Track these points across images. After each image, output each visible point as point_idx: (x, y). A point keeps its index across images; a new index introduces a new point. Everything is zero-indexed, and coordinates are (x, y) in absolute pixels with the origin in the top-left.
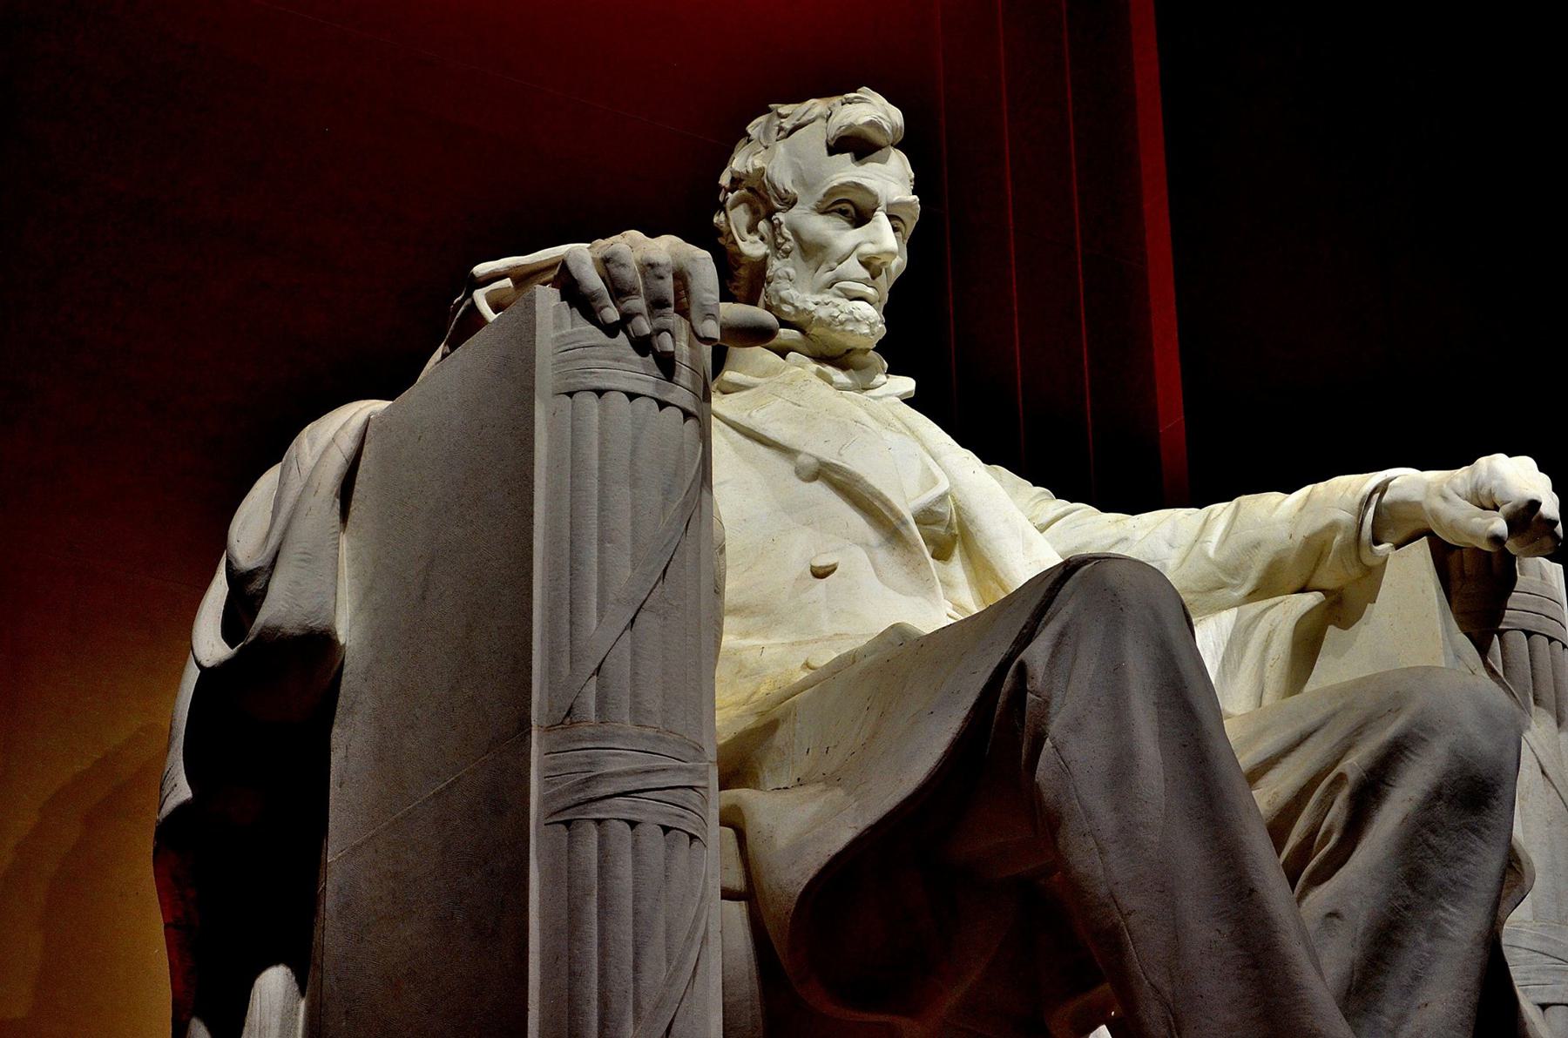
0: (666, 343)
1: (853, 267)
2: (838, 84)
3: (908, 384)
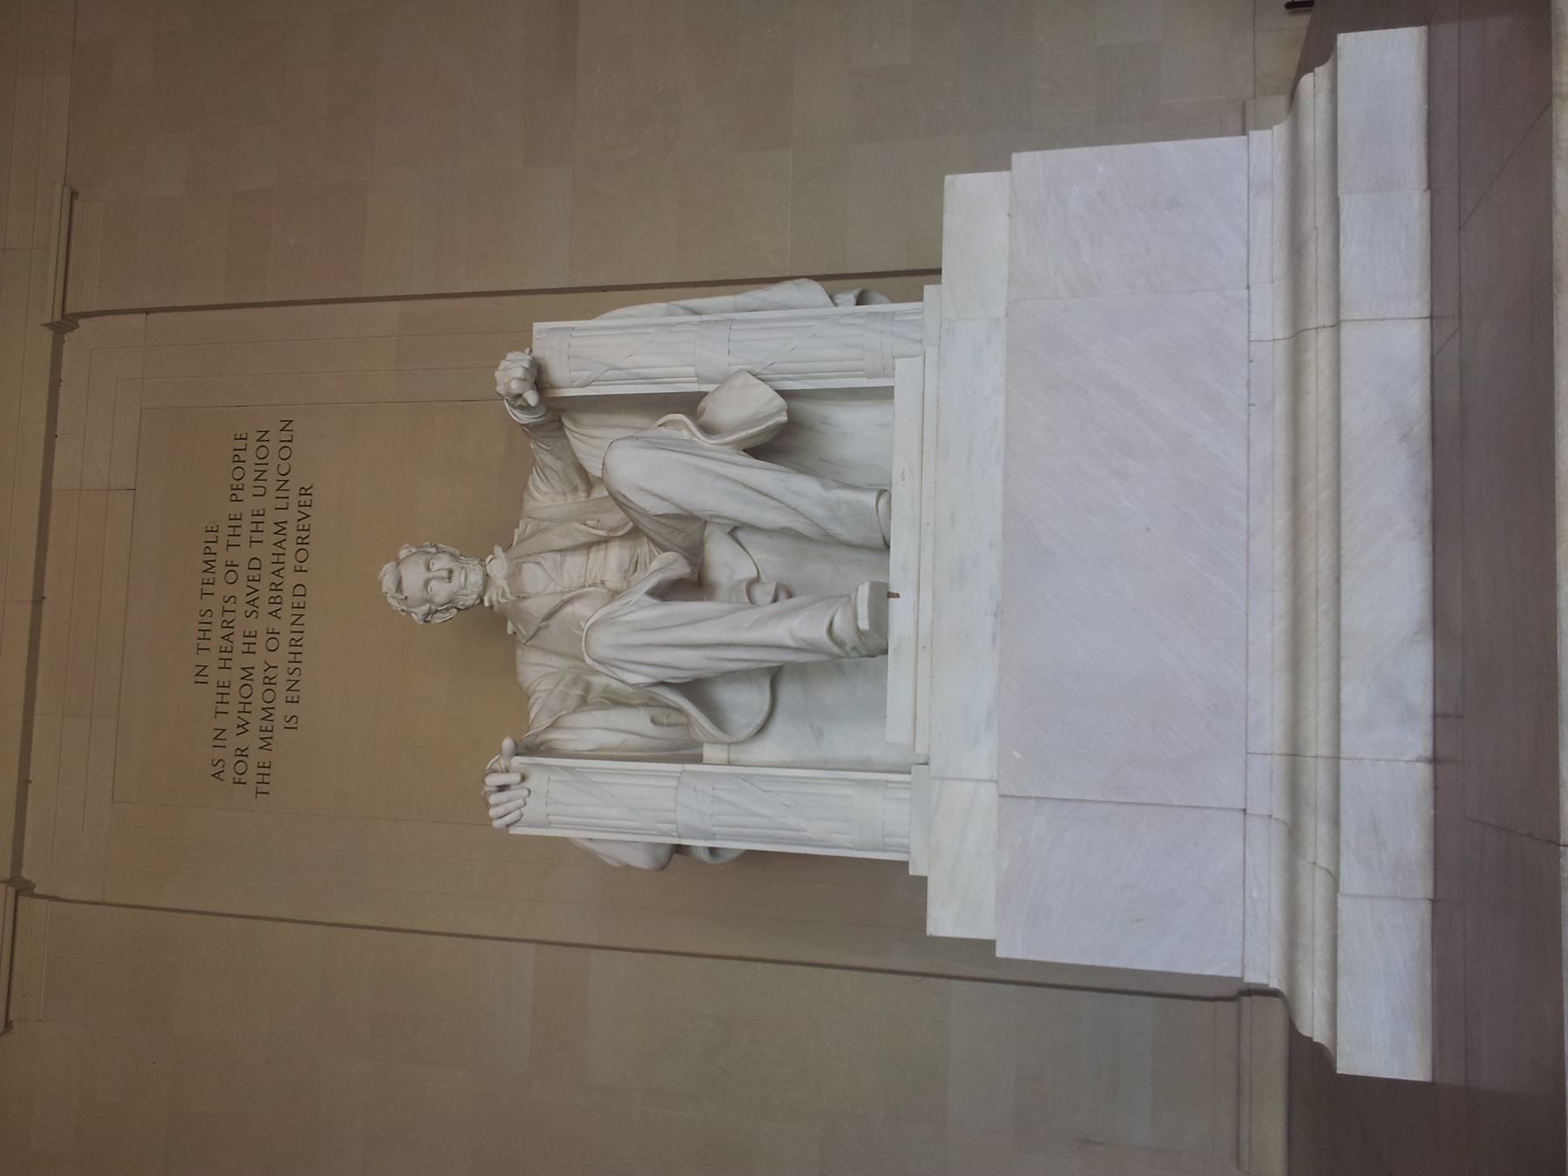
3: (498, 550)
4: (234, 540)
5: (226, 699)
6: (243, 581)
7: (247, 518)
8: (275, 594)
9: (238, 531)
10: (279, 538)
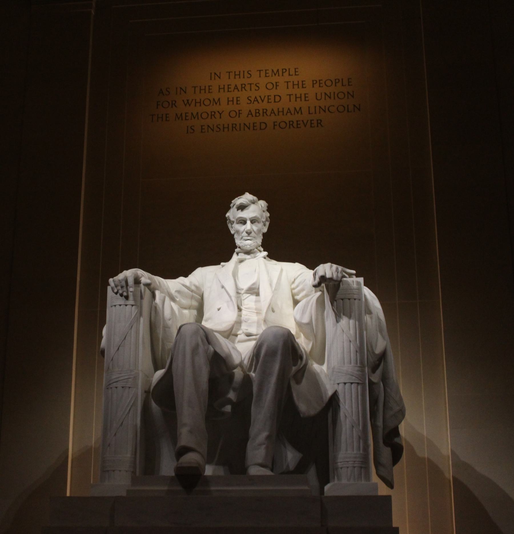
0: (125, 294)
1: (245, 234)
2: (241, 193)
4: (290, 85)
5: (203, 91)
6: (268, 93)
7: (303, 91)
8: (261, 112)
9: (296, 87)
10: (293, 112)
